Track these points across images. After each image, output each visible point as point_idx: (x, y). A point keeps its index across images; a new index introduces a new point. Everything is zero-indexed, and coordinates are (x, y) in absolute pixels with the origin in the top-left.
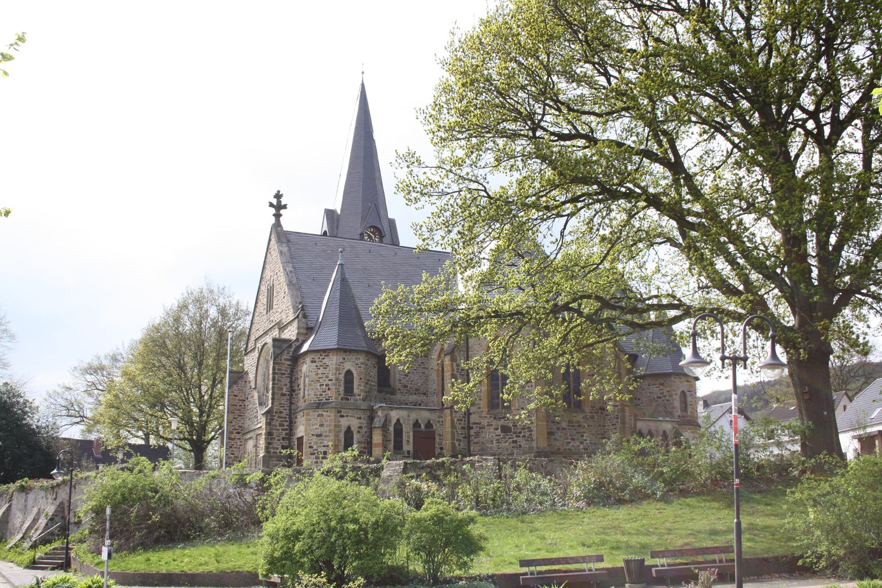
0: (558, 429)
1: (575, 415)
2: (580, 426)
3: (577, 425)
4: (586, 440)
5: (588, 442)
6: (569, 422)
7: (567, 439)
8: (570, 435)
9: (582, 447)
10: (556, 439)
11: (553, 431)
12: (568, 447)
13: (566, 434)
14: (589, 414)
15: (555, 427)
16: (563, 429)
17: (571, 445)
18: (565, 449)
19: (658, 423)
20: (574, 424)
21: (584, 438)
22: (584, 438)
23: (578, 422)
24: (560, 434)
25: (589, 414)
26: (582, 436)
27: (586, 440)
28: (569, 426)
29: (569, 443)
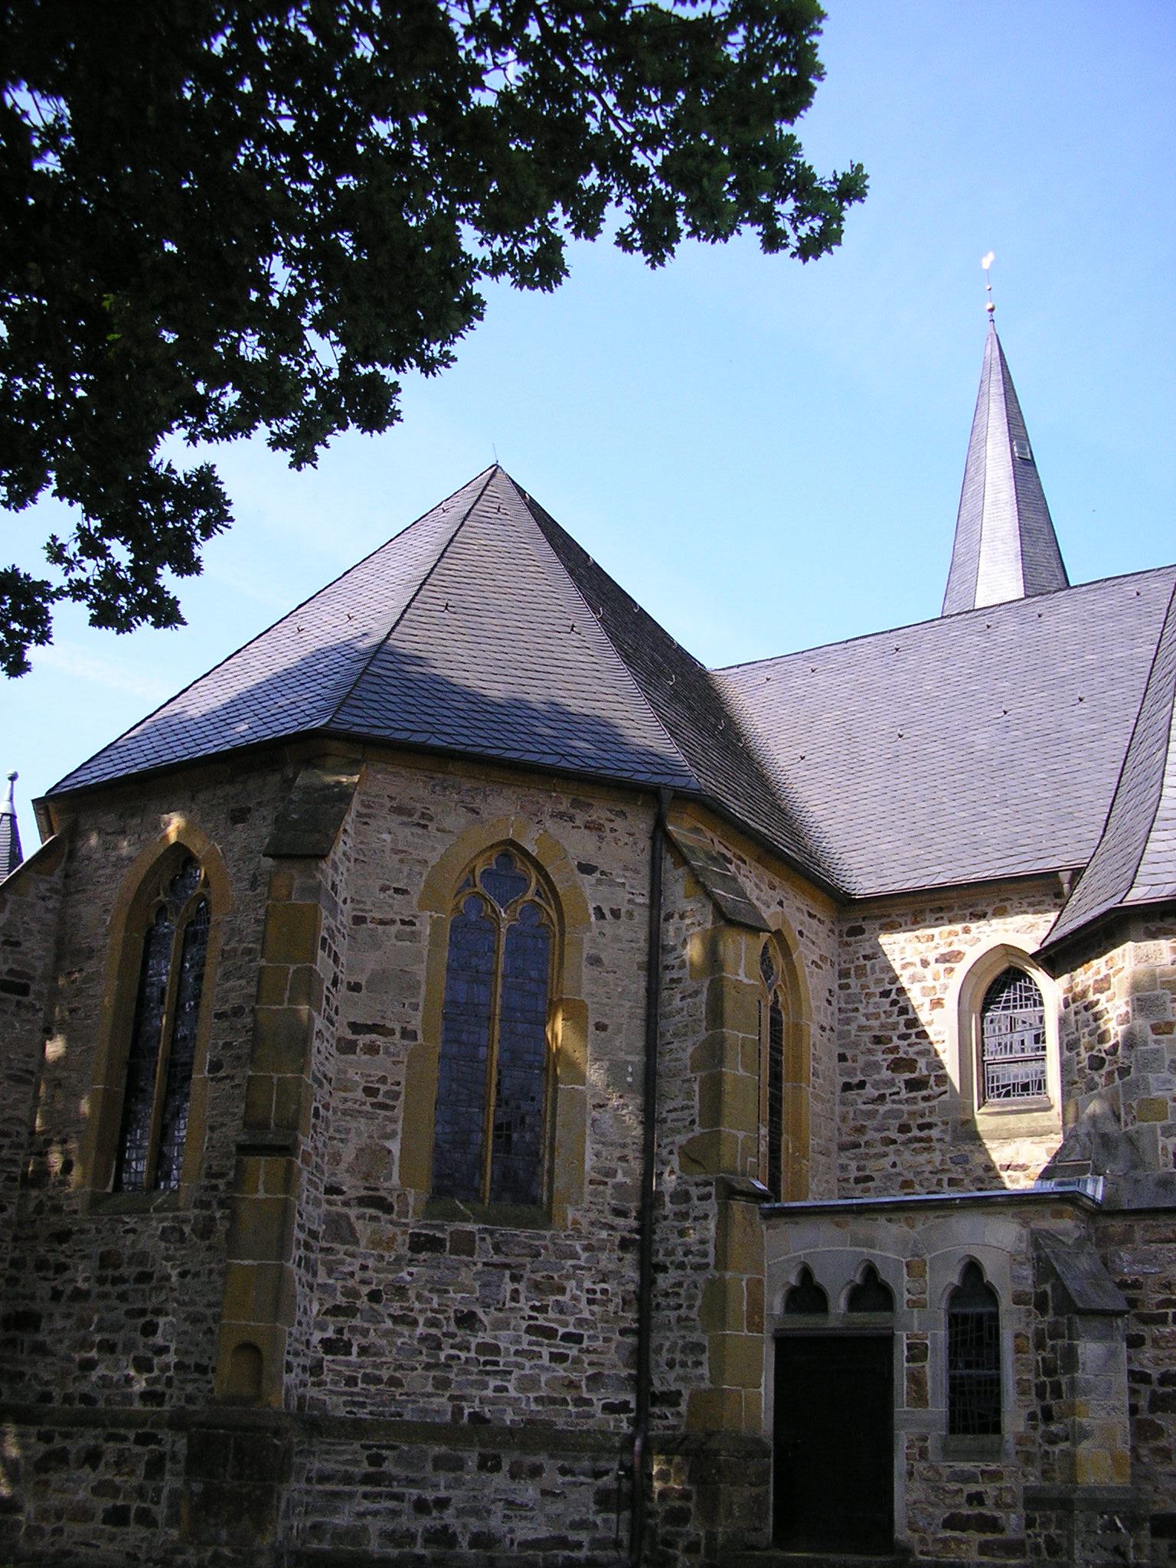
0: (56, 1295)
1: (131, 1221)
2: (144, 1277)
3: (129, 1271)
4: (162, 1350)
5: (172, 1358)
6: (107, 1260)
7: (84, 1344)
8: (99, 1329)
9: (140, 1385)
10: (41, 1349)
11: (36, 1306)
12: (85, 1388)
13: (83, 1323)
14: (192, 1213)
15: (44, 1290)
16: (79, 1295)
17: (94, 1376)
18: (68, 1399)
19: (923, 1223)
20: (126, 1271)
21: (159, 1340)
22: (159, 1340)
23: (141, 1258)
24: (59, 1323)
25: (192, 1213)
26: (150, 1329)
27: (162, 1350)
28: (101, 1281)
29: (89, 1365)
